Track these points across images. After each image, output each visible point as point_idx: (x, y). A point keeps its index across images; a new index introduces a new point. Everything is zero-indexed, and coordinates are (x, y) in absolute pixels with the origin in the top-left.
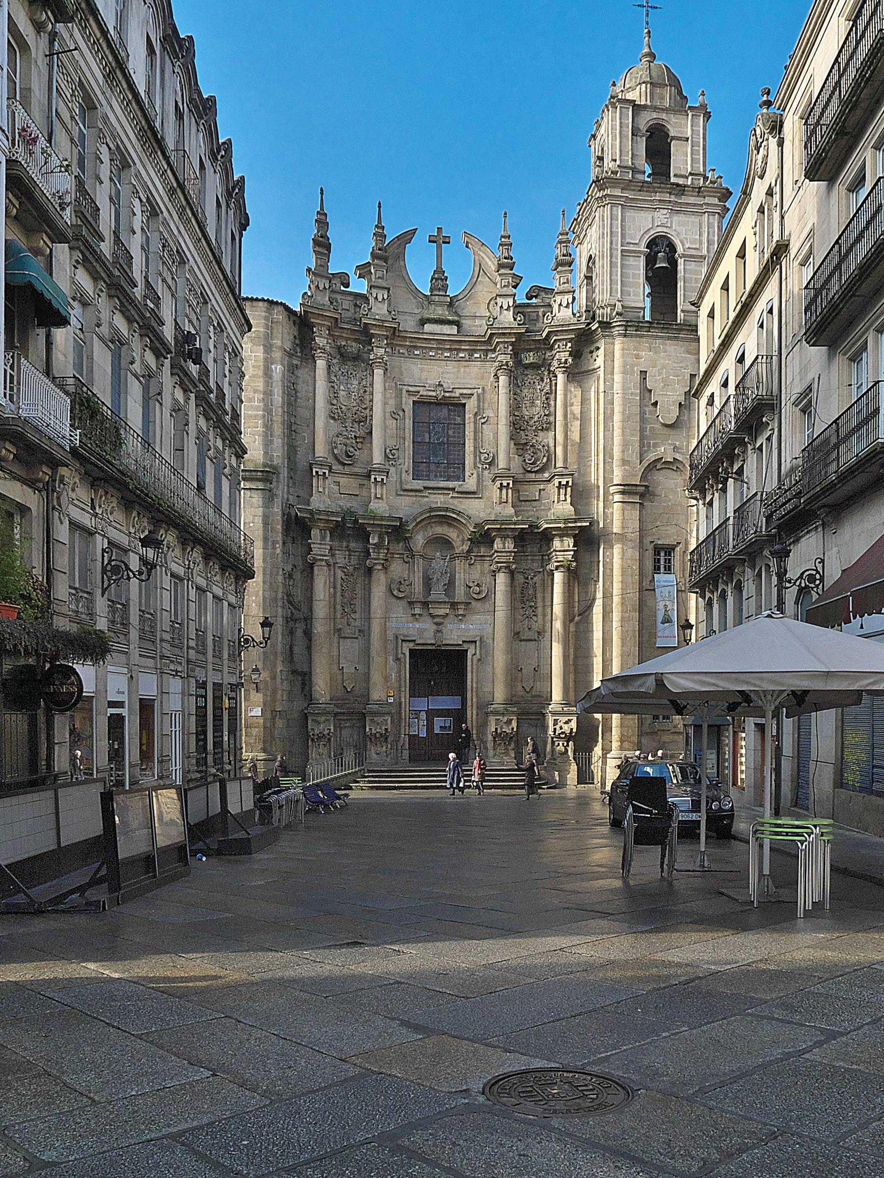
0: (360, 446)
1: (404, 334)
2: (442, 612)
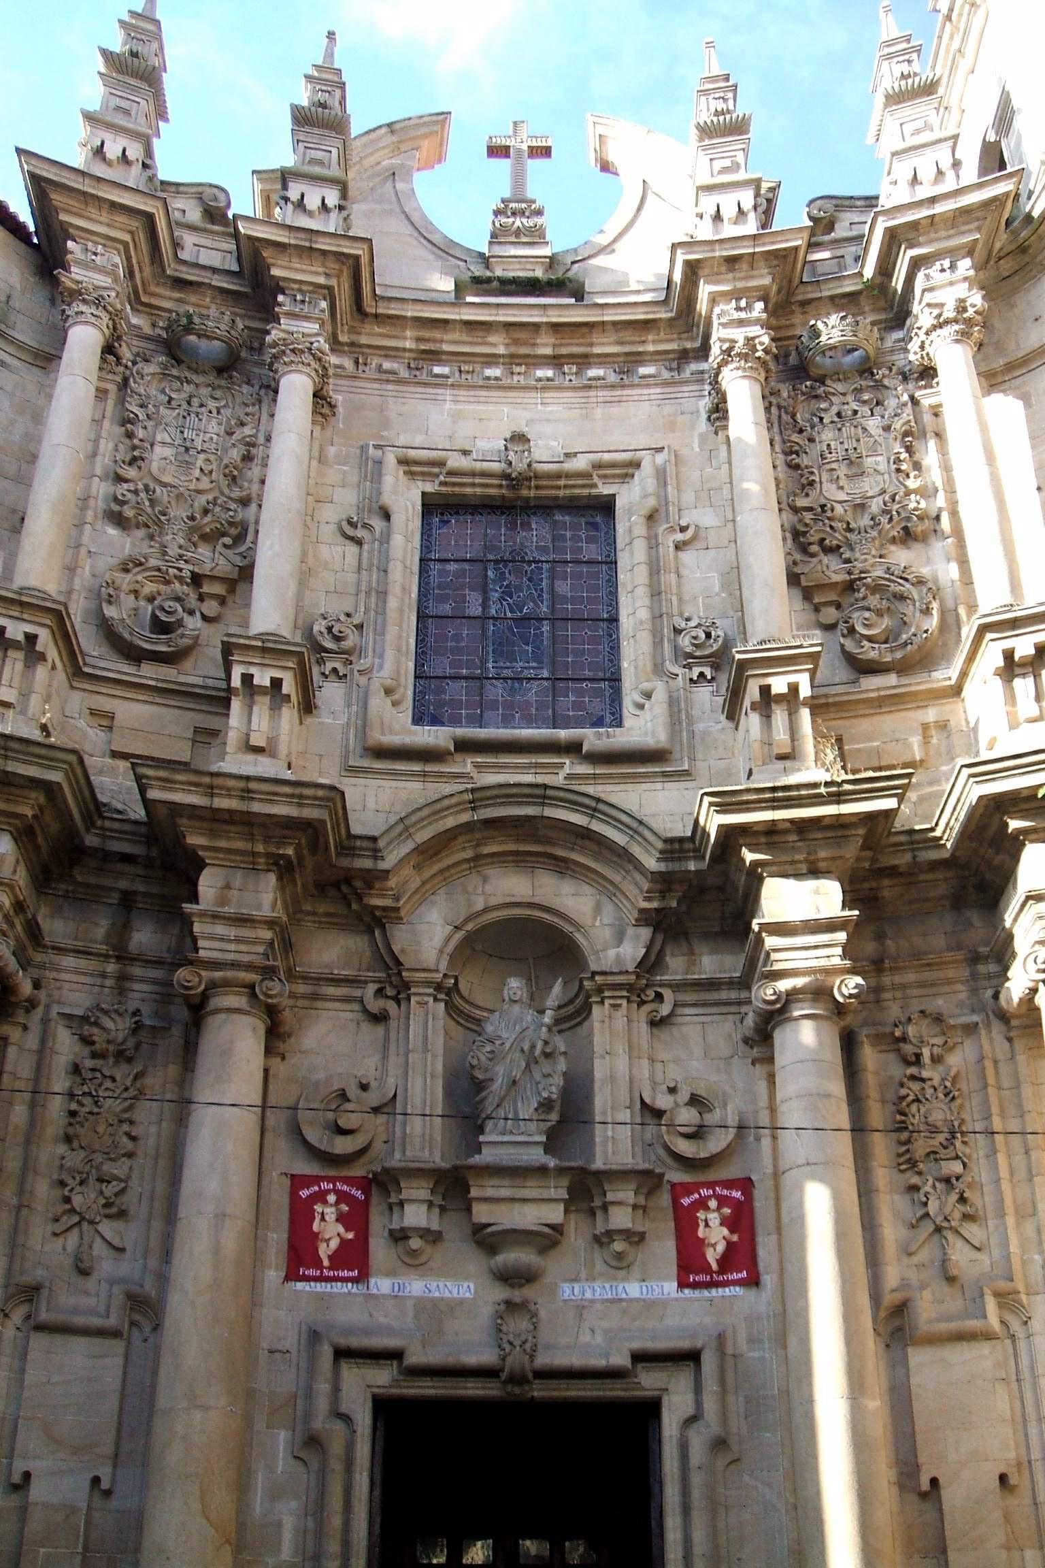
2: (529, 1217)
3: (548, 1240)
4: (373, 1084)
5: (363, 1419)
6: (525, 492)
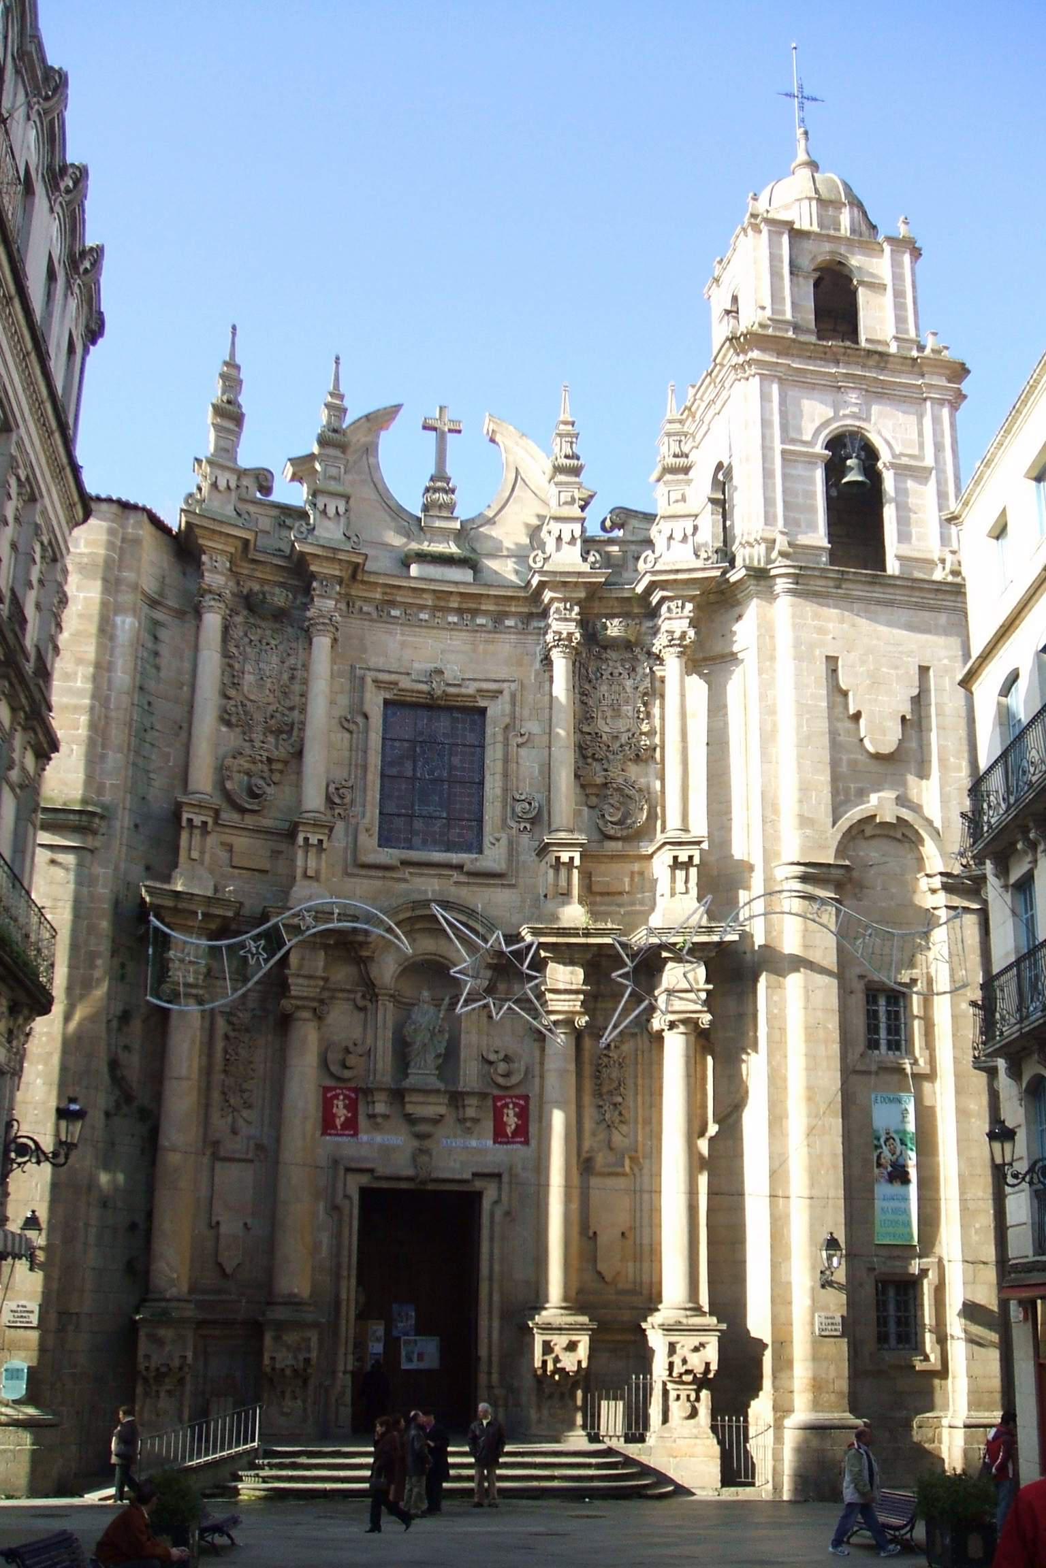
0: (276, 777)
1: (372, 579)
2: (430, 1111)
5: (356, 1197)
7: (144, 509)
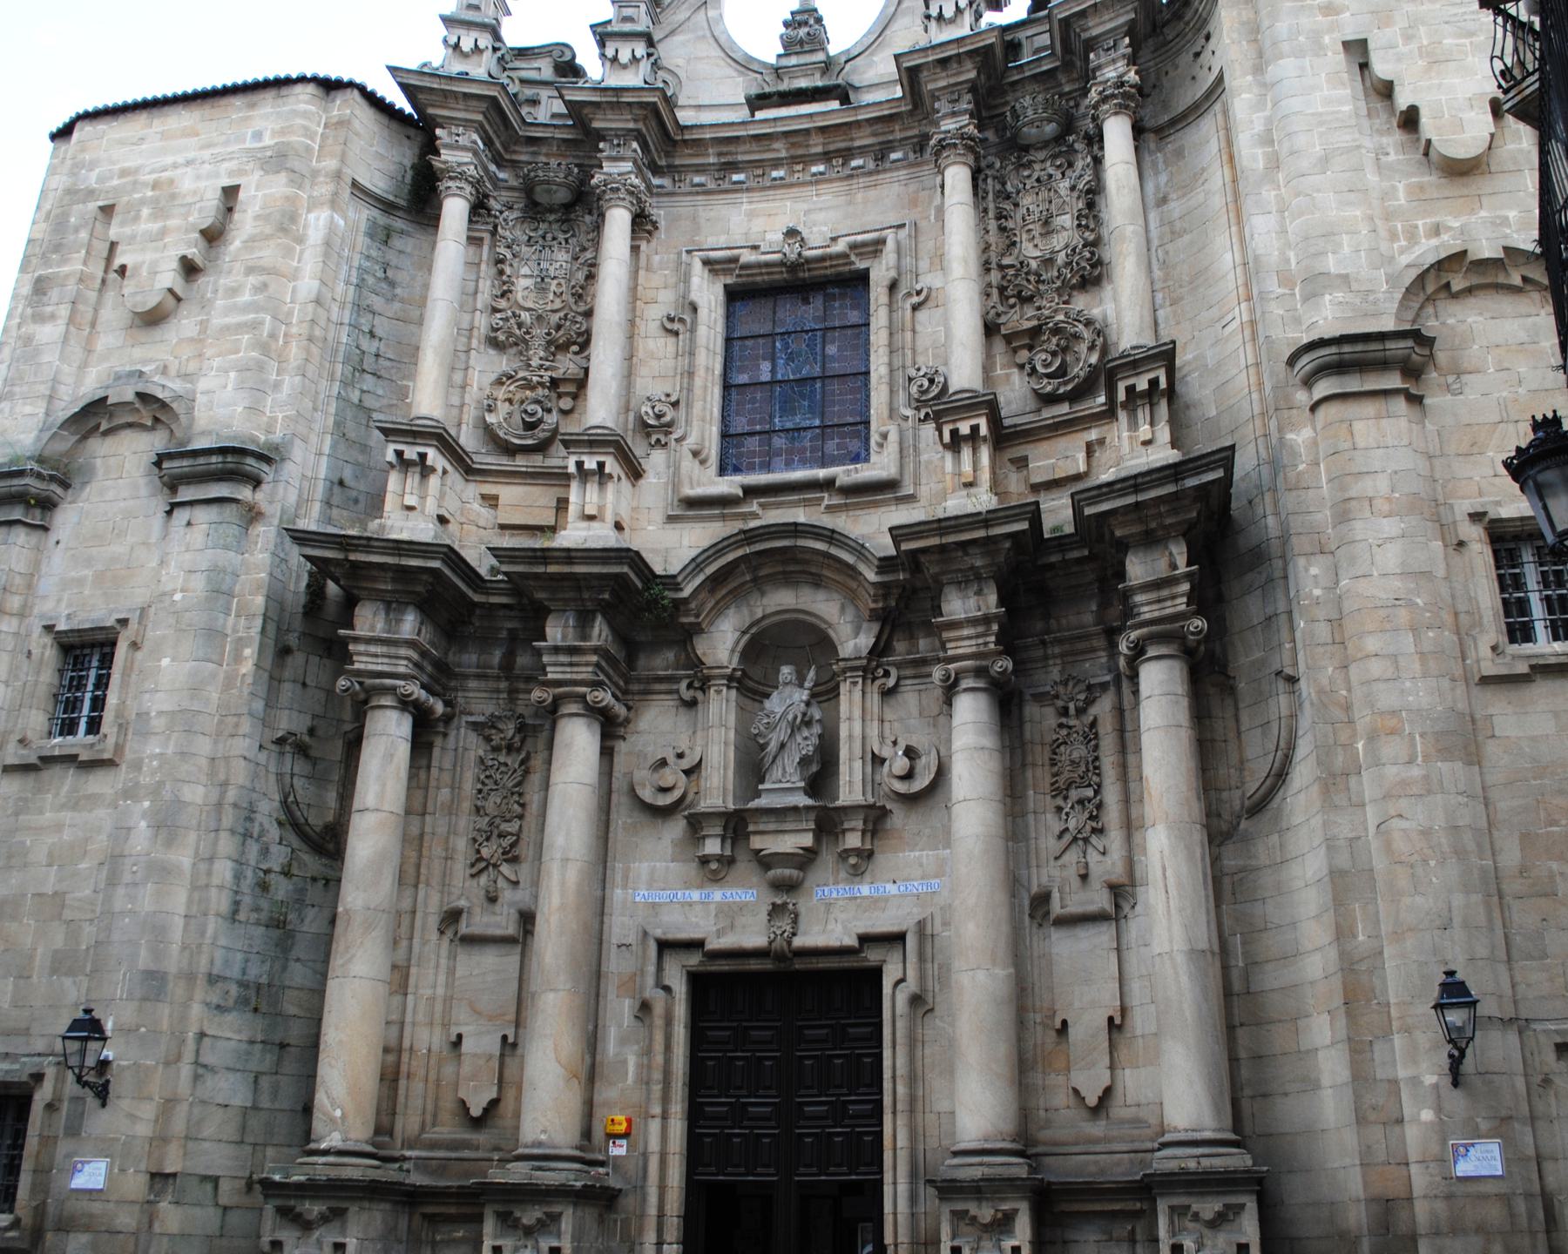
2: (790, 843)
3: (806, 859)
4: (687, 752)
6: (801, 275)
7: (351, 85)
